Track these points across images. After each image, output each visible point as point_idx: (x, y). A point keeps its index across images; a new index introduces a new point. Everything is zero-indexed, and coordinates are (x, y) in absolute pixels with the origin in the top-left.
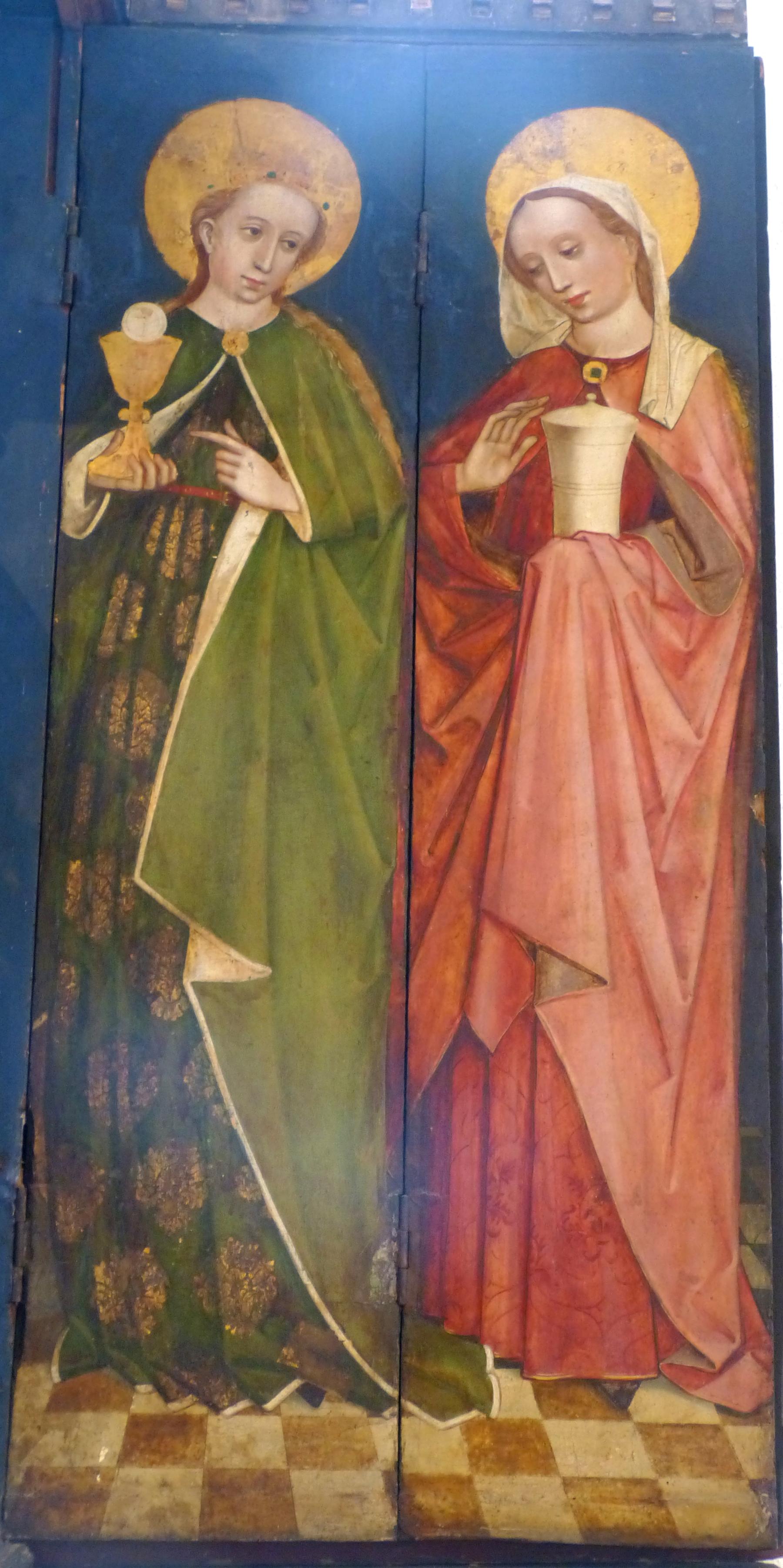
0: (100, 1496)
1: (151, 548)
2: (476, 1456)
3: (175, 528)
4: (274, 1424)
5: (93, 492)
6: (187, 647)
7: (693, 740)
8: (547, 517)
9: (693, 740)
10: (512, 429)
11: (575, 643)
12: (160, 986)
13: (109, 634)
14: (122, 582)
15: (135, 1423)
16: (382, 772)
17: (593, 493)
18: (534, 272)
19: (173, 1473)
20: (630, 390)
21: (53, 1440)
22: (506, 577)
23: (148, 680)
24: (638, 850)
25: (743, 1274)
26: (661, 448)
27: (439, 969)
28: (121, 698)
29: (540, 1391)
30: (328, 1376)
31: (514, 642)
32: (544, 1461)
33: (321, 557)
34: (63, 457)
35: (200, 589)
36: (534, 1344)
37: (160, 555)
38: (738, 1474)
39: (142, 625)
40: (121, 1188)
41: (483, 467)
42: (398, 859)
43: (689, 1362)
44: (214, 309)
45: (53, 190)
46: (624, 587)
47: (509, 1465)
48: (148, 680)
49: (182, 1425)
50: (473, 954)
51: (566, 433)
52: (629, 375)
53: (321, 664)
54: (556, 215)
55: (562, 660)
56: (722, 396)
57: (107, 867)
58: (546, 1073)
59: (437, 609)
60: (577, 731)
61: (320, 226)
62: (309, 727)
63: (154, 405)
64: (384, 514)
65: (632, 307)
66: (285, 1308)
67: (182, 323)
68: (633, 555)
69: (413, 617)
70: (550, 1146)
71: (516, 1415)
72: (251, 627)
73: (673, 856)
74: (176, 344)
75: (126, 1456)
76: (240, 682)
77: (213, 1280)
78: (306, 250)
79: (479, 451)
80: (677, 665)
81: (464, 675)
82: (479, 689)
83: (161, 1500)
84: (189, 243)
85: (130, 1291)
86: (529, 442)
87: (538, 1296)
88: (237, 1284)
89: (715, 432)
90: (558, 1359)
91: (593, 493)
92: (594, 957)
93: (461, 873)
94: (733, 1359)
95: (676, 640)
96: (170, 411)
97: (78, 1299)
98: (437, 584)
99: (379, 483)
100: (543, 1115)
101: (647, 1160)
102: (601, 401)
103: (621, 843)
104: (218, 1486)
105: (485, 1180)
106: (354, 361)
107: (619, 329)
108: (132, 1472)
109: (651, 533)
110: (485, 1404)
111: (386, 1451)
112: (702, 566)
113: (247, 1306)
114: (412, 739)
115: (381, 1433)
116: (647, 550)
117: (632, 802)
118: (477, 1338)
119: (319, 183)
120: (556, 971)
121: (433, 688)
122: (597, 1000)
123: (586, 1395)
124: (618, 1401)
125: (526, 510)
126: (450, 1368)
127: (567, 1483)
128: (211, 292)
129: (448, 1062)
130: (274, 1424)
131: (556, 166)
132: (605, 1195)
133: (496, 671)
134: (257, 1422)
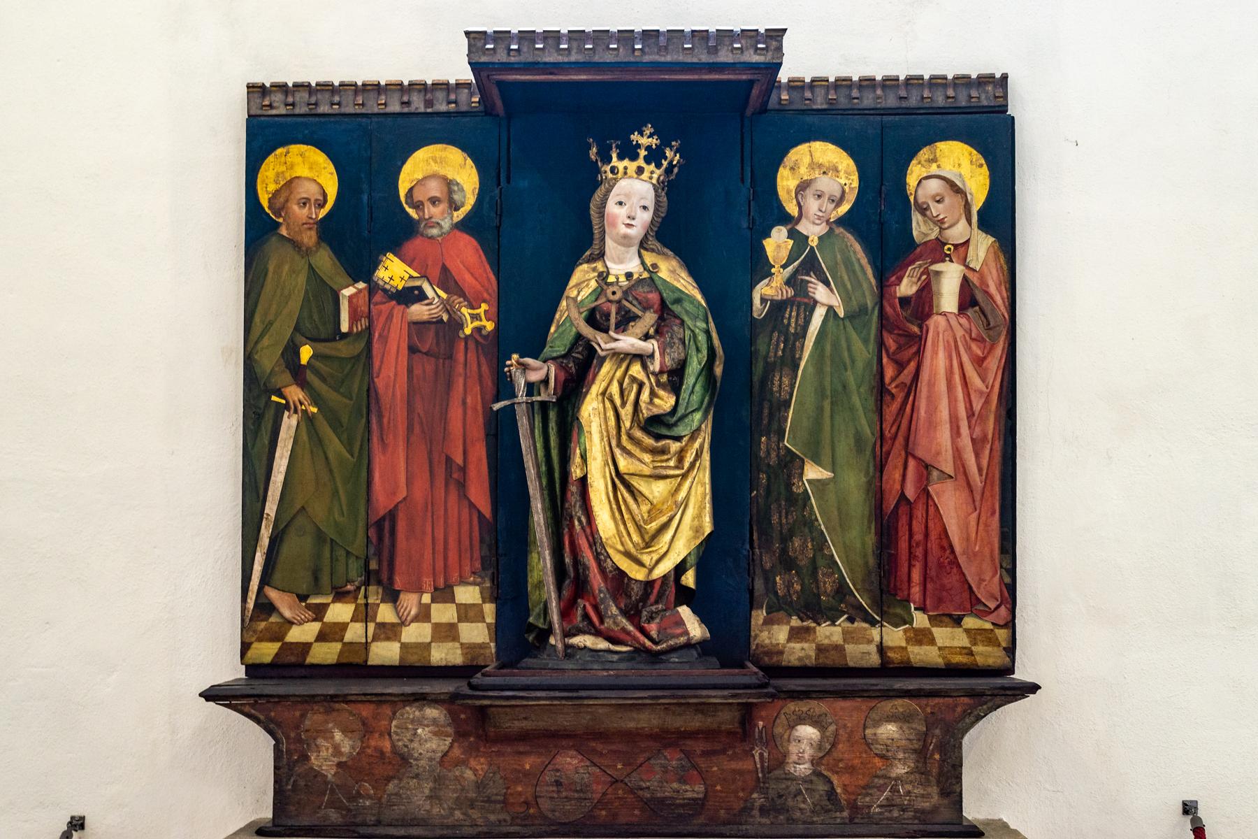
0: (781, 653)
1: (785, 321)
2: (908, 640)
3: (794, 314)
4: (839, 629)
5: (763, 300)
6: (800, 359)
7: (984, 389)
8: (931, 307)
9: (984, 389)
10: (917, 273)
11: (941, 355)
12: (795, 481)
13: (772, 354)
14: (776, 335)
15: (792, 629)
16: (871, 403)
17: (948, 298)
18: (926, 209)
19: (806, 645)
20: (962, 256)
21: (765, 634)
22: (916, 329)
23: (786, 371)
24: (965, 430)
25: (1001, 576)
26: (974, 279)
27: (893, 474)
28: (777, 378)
29: (930, 618)
30: (857, 613)
31: (919, 353)
32: (932, 642)
33: (847, 323)
34: (752, 287)
35: (804, 337)
36: (928, 602)
37: (789, 324)
38: (999, 645)
39: (783, 351)
40: (784, 551)
41: (907, 287)
42: (877, 434)
43: (982, 608)
44: (803, 228)
45: (743, 180)
46: (960, 333)
47: (920, 643)
48: (786, 371)
49: (808, 630)
50: (905, 468)
51: (938, 273)
52: (962, 250)
53: (848, 361)
54: (934, 186)
55: (937, 362)
56: (997, 258)
57: (774, 439)
58: (932, 509)
59: (891, 342)
60: (942, 386)
61: (843, 192)
62: (844, 387)
63: (784, 267)
64: (870, 305)
65: (963, 222)
66: (842, 590)
67: (793, 234)
68: (963, 321)
69: (881, 344)
70: (933, 536)
71: (922, 626)
72: (823, 350)
73: (978, 432)
74: (791, 242)
75: (789, 640)
76: (819, 371)
77: (816, 581)
78: (839, 203)
79: (905, 281)
80: (979, 362)
81: (901, 366)
82: (906, 372)
83: (802, 654)
84: (795, 202)
85: (789, 585)
86: (924, 277)
87: (929, 586)
88: (825, 583)
89: (994, 272)
90: (936, 608)
91: (948, 298)
92: (949, 469)
93: (900, 439)
94: (998, 607)
95: (979, 353)
96: (790, 269)
97: (770, 587)
98: (890, 332)
99: (867, 293)
100: (931, 524)
101: (968, 539)
102: (951, 261)
103: (958, 428)
104: (821, 649)
105: (910, 547)
106: (858, 247)
107: (959, 231)
108: (792, 645)
109: (970, 312)
110: (911, 623)
111: (877, 638)
112: (989, 324)
113: (829, 589)
114: (881, 392)
115: (875, 633)
116: (968, 318)
117: (962, 413)
118: (908, 601)
119: (842, 174)
120: (935, 473)
121: (889, 372)
122: (949, 484)
123: (946, 619)
124: (957, 621)
125: (922, 305)
126: (899, 611)
127: (940, 649)
128: (804, 221)
129: (897, 507)
130: (839, 629)
131: (934, 166)
132: (953, 552)
133: (913, 365)
134: (833, 629)
